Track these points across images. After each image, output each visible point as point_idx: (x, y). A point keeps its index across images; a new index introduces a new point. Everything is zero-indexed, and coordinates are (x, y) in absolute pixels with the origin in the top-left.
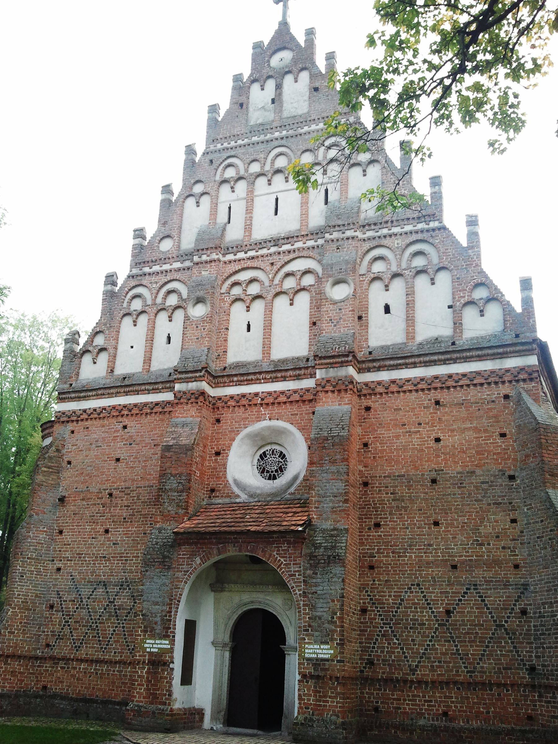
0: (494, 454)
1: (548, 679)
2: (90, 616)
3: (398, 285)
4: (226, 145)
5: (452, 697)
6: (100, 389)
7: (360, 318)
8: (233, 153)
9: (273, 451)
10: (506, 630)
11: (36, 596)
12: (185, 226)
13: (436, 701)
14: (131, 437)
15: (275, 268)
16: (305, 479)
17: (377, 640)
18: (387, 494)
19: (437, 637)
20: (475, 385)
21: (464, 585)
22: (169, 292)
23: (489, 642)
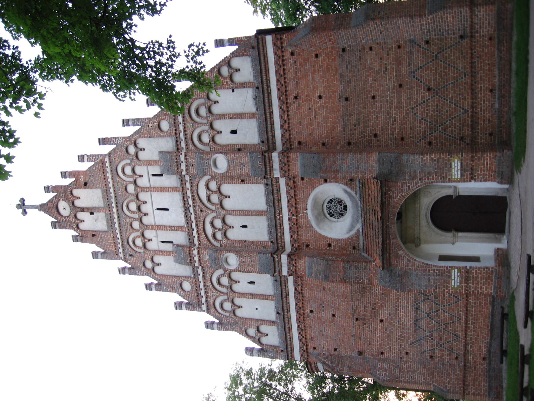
0: (329, 61)
1: (467, 27)
2: (437, 329)
3: (218, 125)
4: (120, 246)
5: (481, 87)
6: (285, 330)
7: (239, 150)
8: (125, 241)
9: (328, 208)
10: (438, 53)
11: (425, 368)
12: (174, 273)
13: (484, 97)
14: (318, 307)
15: (204, 209)
16: (346, 184)
17: (448, 135)
18: (355, 129)
19: (444, 96)
20: (284, 74)
21: (412, 80)
22: (219, 283)
23: (446, 64)
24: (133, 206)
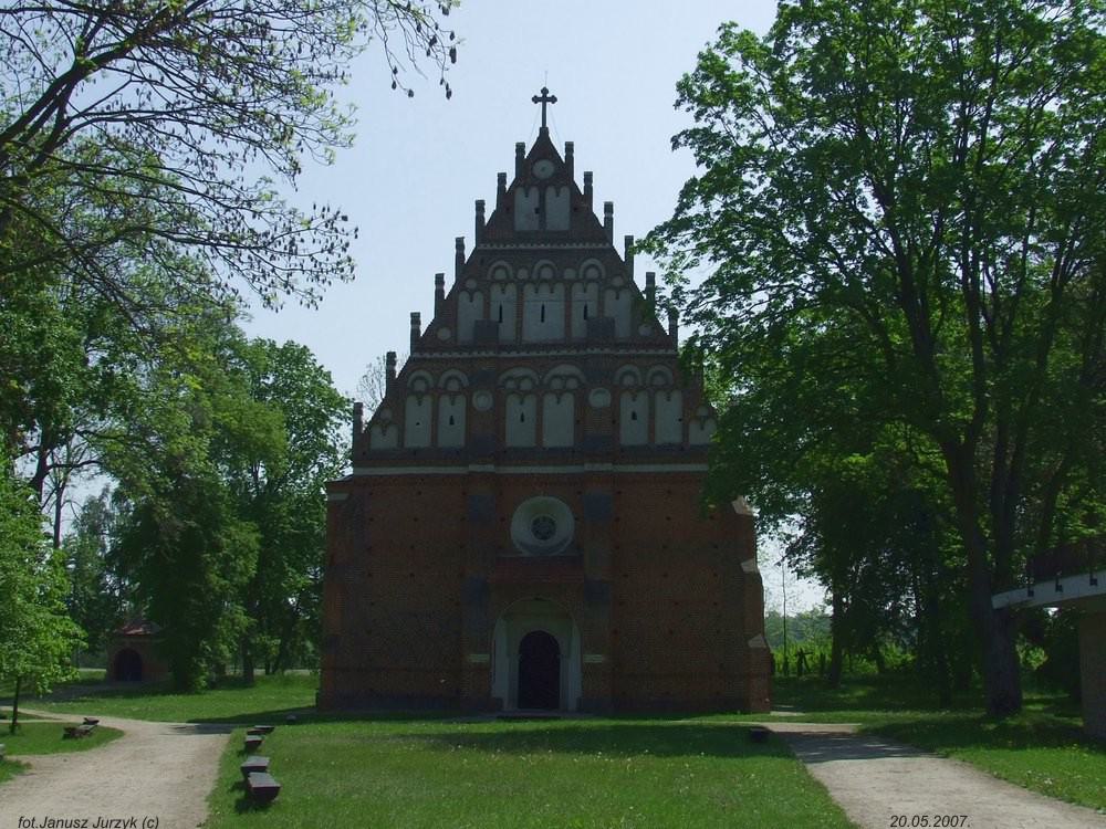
4: (495, 247)
7: (614, 422)
24: (547, 274)
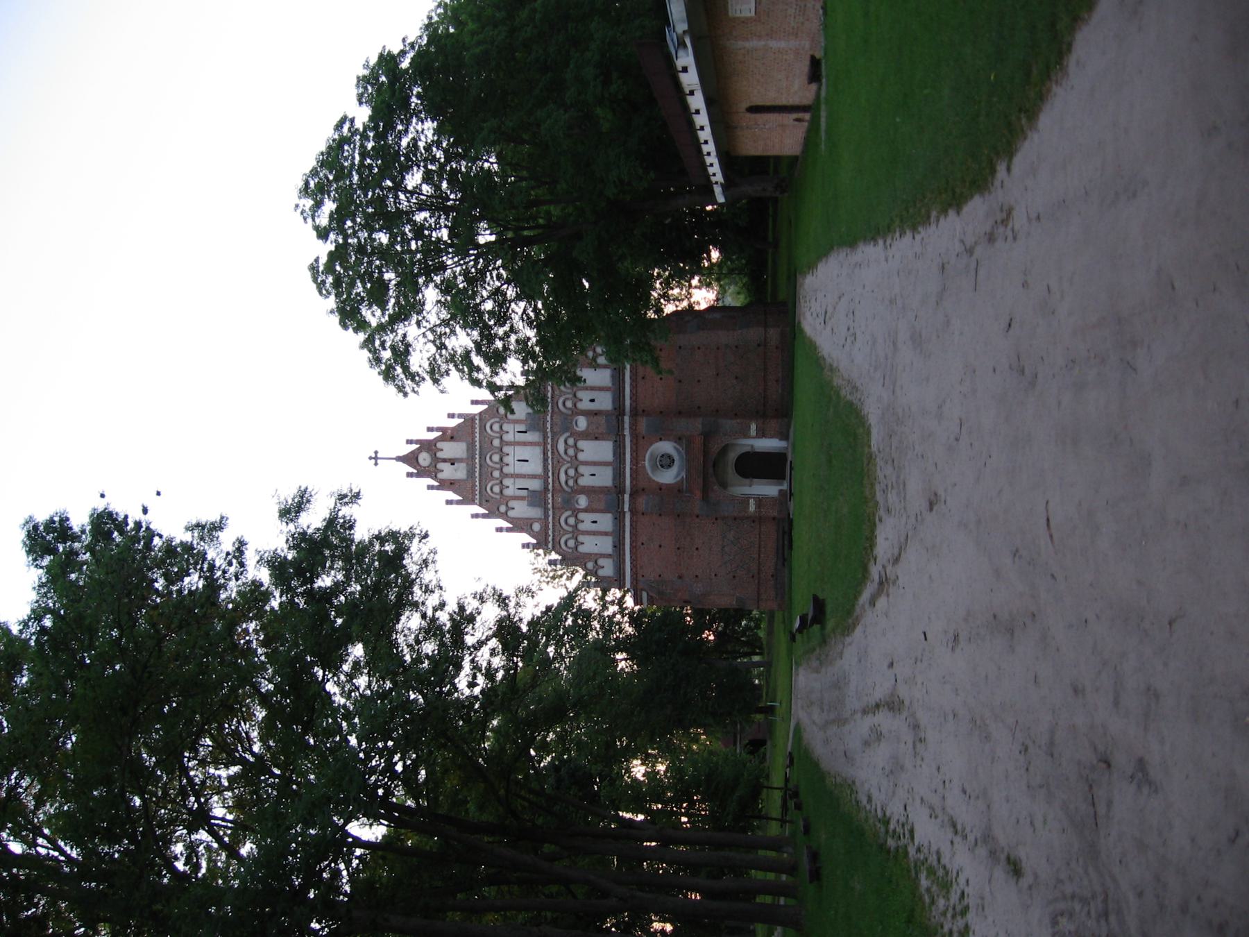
24: (496, 458)
